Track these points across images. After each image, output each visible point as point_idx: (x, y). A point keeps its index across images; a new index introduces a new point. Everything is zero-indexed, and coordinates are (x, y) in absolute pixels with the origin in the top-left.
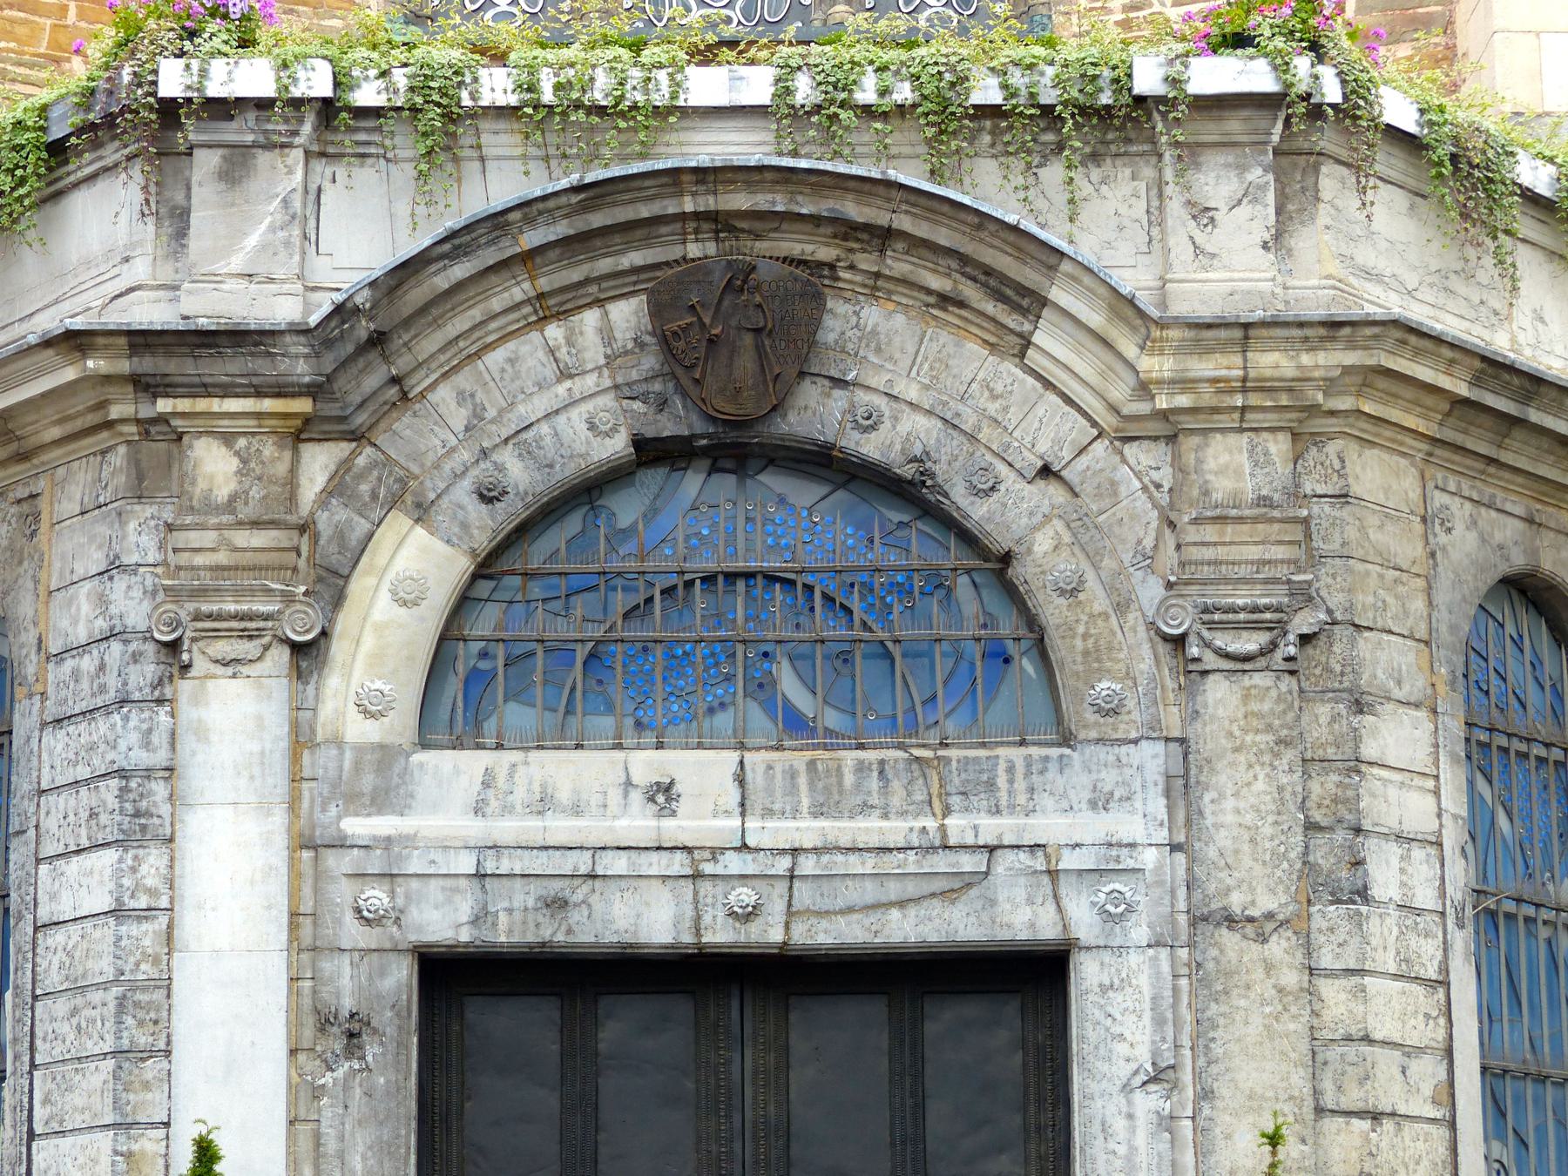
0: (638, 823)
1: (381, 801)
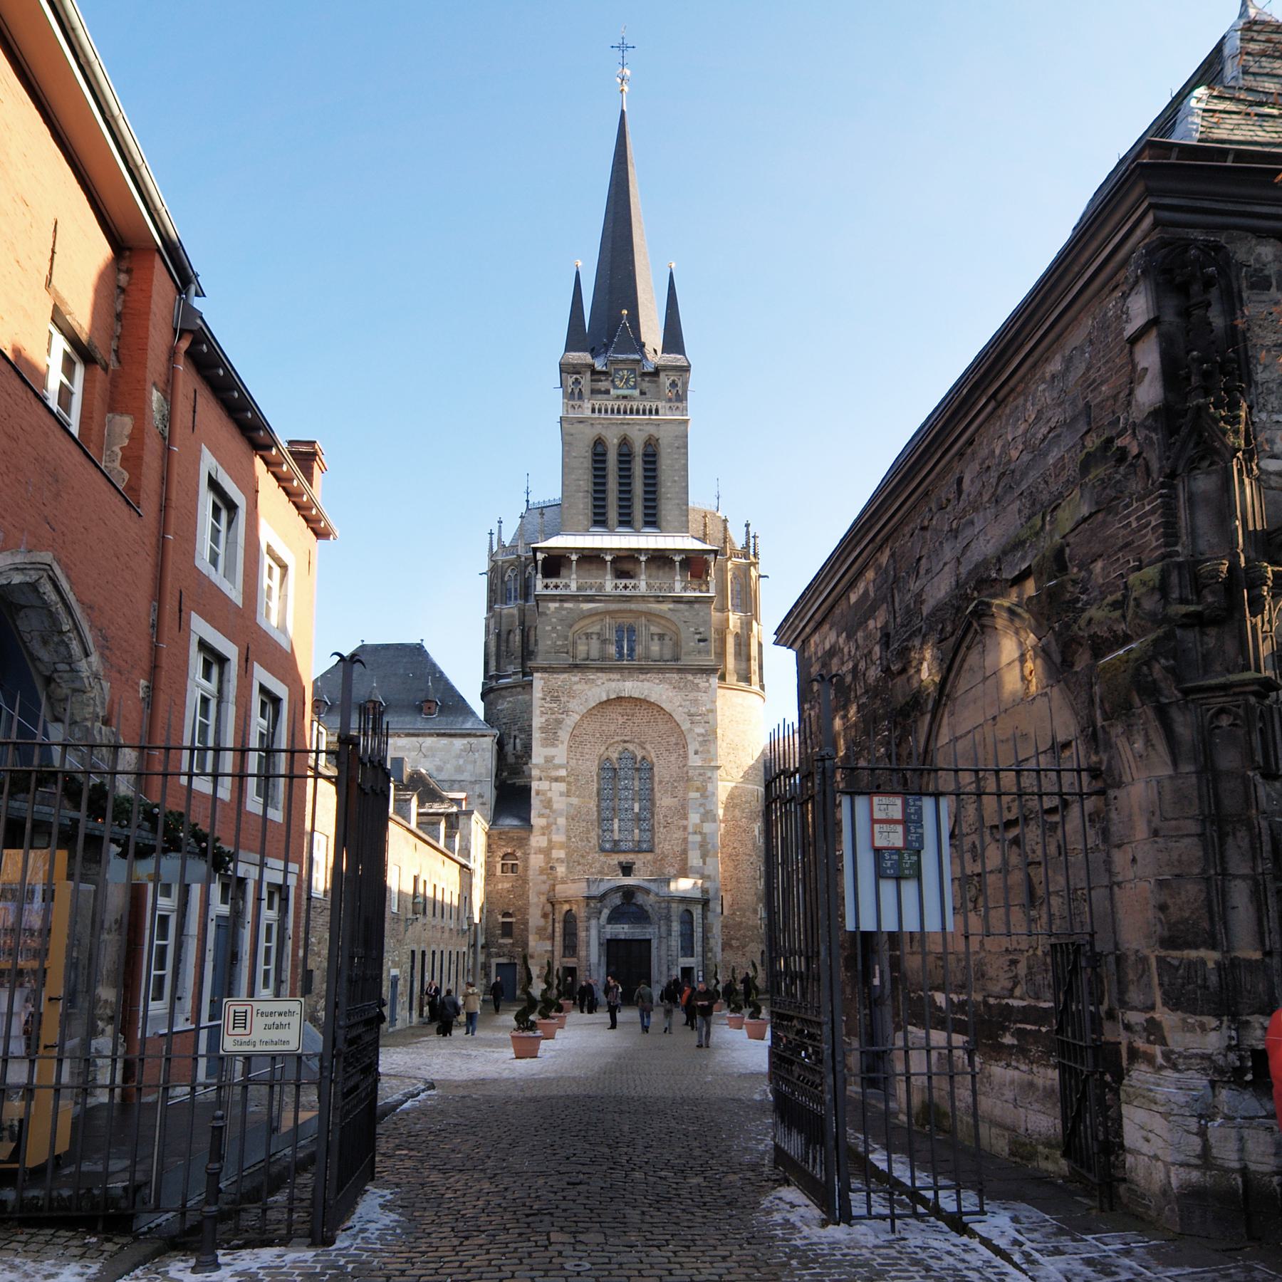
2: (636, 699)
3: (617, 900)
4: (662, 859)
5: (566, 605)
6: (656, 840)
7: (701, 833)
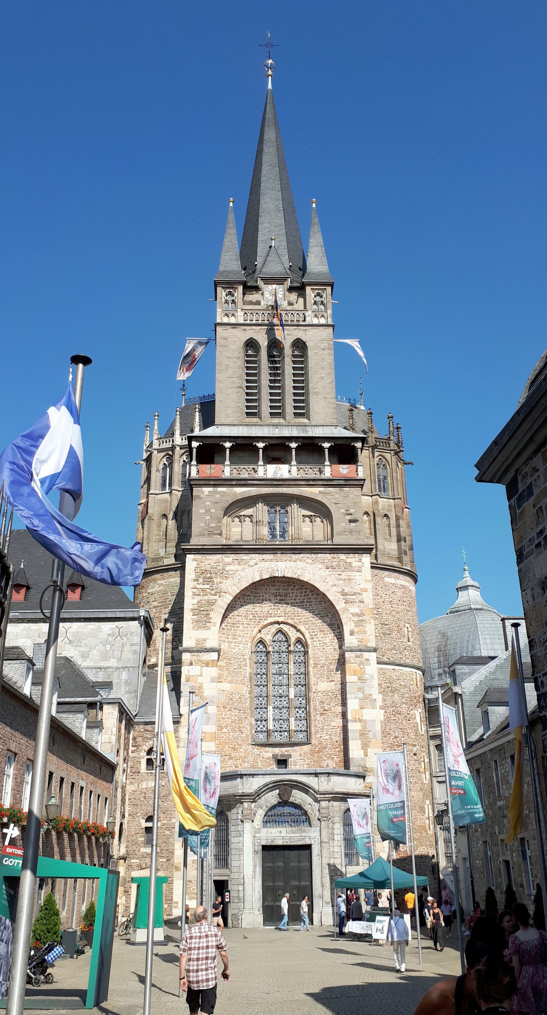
0: (278, 834)
1: (259, 833)
2: (288, 577)
3: (272, 798)
4: (318, 752)
5: (220, 489)
6: (313, 729)
7: (360, 721)
